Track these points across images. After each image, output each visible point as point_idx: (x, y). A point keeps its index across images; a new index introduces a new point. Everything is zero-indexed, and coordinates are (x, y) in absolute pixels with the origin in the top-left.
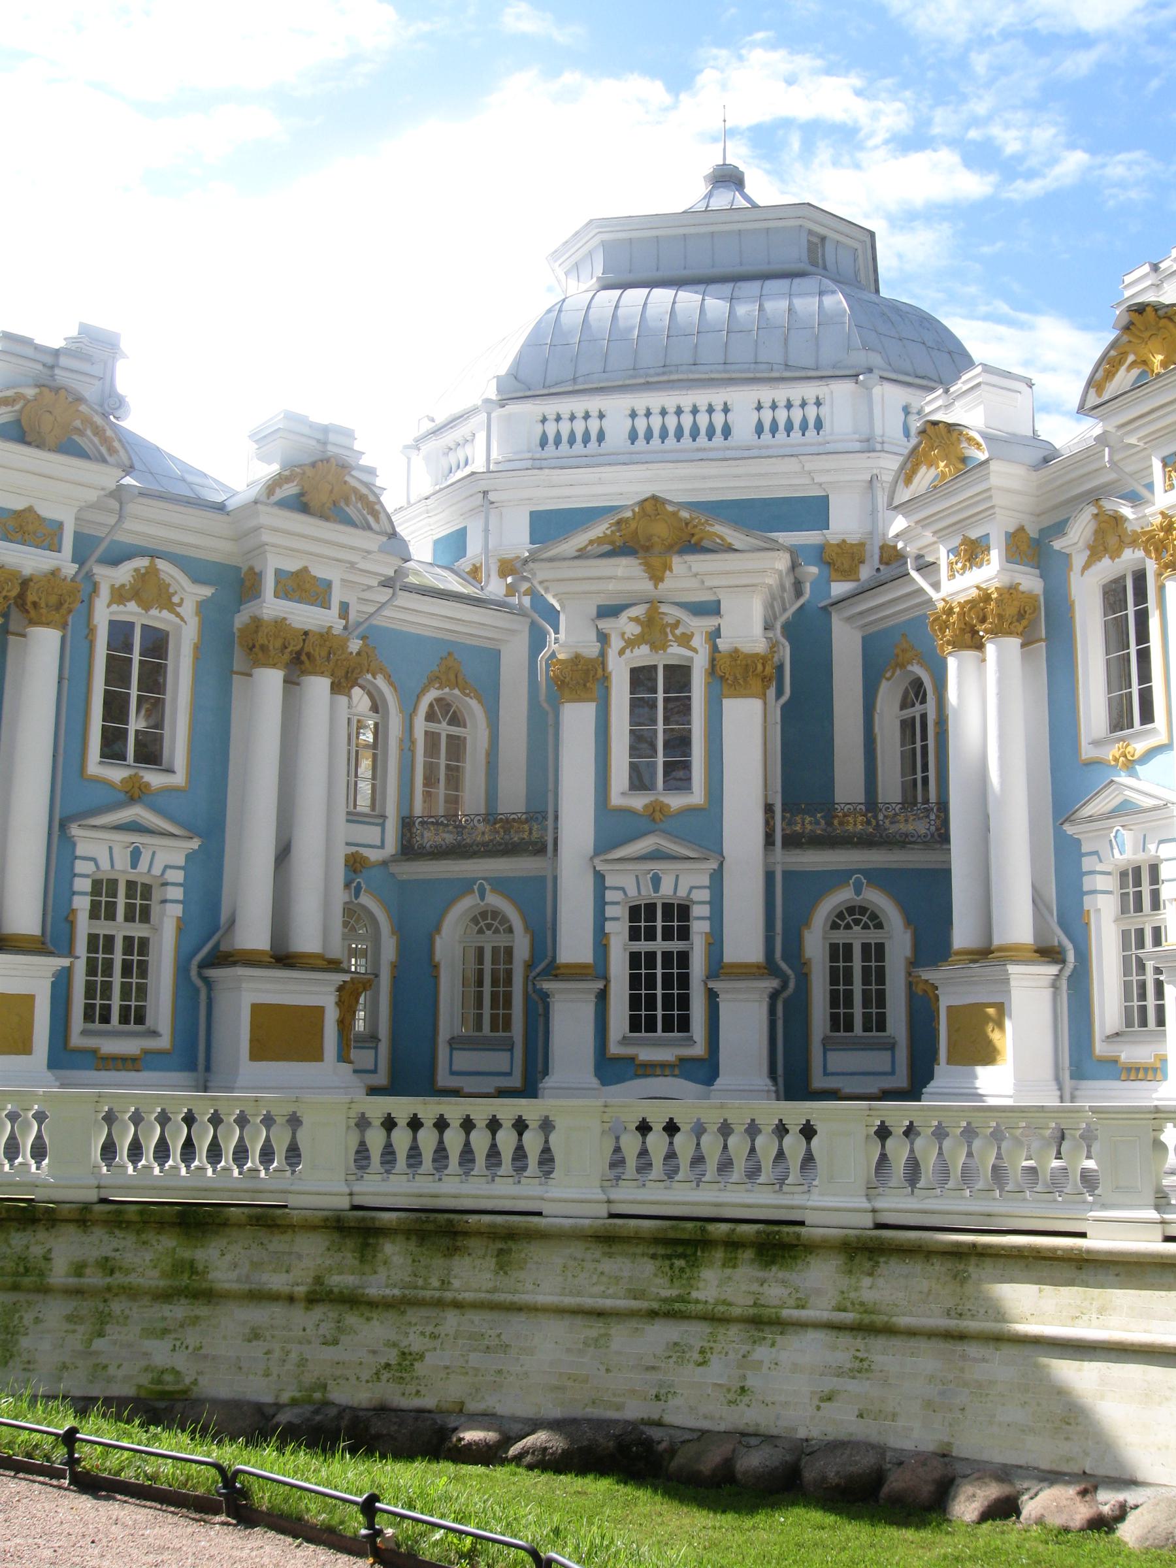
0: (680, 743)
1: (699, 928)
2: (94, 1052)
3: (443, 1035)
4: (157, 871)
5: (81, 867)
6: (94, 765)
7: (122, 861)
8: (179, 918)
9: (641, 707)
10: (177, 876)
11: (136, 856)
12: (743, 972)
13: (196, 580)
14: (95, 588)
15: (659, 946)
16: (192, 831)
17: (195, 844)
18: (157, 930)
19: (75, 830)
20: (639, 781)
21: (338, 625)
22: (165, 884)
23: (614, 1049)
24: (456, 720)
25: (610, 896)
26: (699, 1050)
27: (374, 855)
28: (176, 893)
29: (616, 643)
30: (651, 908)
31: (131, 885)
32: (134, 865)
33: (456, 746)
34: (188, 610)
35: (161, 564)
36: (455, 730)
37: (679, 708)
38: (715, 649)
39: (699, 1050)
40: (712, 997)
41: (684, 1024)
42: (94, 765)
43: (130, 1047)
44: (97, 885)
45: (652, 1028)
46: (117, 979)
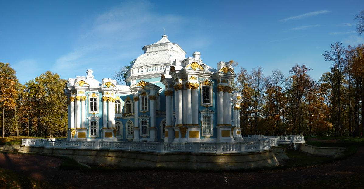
0: (146, 105)
1: (148, 123)
3: (127, 134)
9: (143, 101)
12: (152, 127)
15: (145, 125)
20: (143, 108)
22: (97, 122)
23: (141, 135)
24: (130, 102)
25: (140, 120)
26: (148, 136)
27: (120, 117)
29: (140, 95)
30: (144, 121)
33: (130, 105)
36: (129, 104)
37: (146, 101)
38: (149, 95)
39: (148, 136)
40: (149, 130)
41: (147, 134)
45: (144, 134)
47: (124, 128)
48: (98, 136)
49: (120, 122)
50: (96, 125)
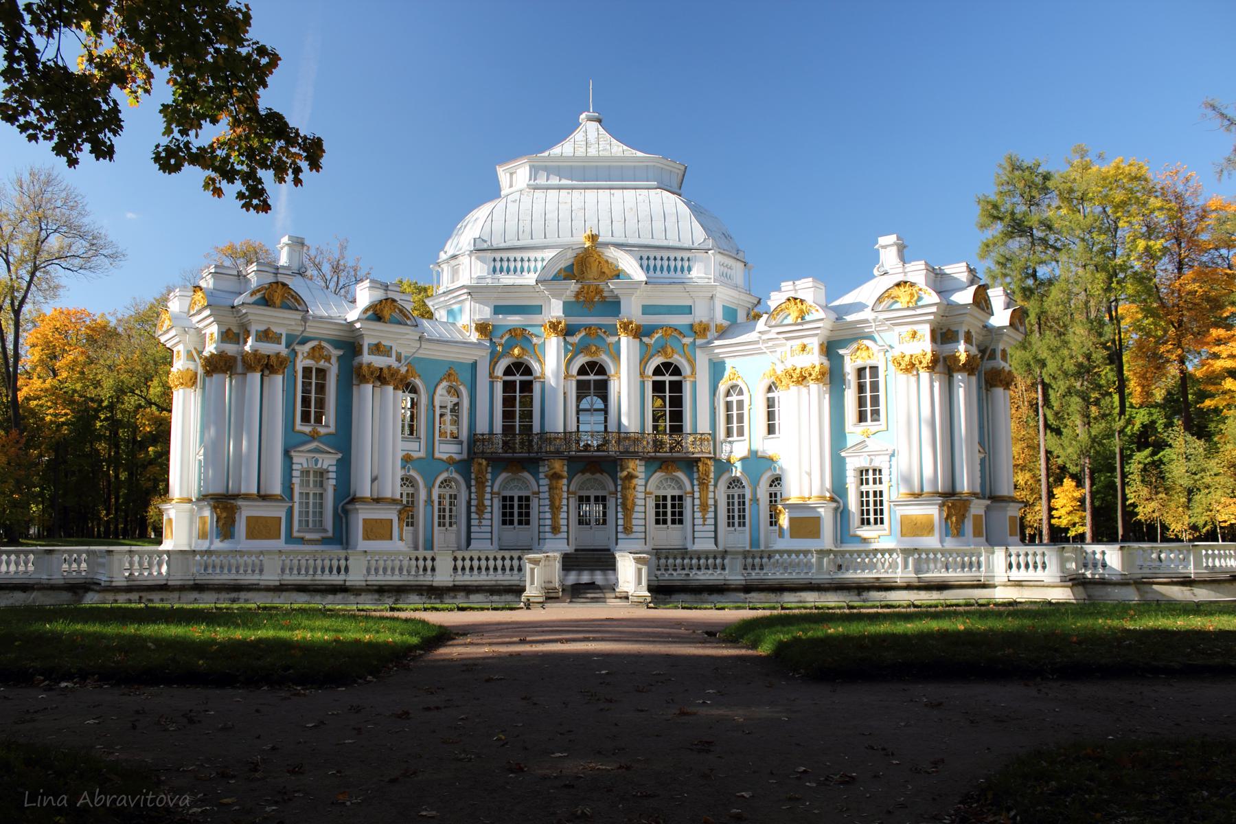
6: (299, 426)
8: (335, 486)
10: (334, 468)
11: (317, 461)
13: (336, 348)
14: (296, 354)
16: (338, 449)
17: (340, 456)
18: (325, 490)
19: (293, 454)
21: (395, 365)
22: (328, 472)
28: (333, 475)
31: (315, 472)
34: (334, 360)
35: (323, 344)
42: (299, 426)
44: (302, 472)
47: (429, 501)
48: (330, 534)
49: (412, 473)
50: (321, 486)
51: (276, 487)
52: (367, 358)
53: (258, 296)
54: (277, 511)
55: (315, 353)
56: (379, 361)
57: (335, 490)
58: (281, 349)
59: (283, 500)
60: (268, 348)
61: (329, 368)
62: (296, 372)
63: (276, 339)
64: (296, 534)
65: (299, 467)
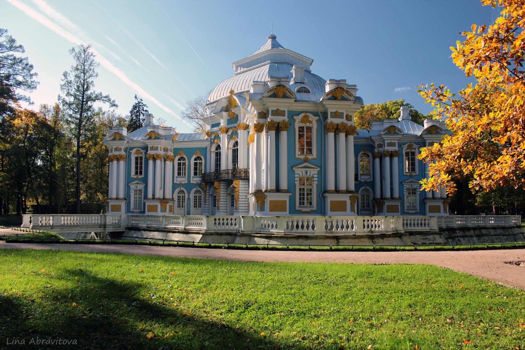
2: (301, 211)
4: (311, 175)
5: (296, 176)
7: (304, 174)
10: (316, 176)
11: (306, 172)
19: (294, 169)
28: (316, 179)
32: (306, 174)
34: (314, 122)
43: (308, 210)
44: (300, 180)
46: (305, 197)
51: (284, 185)
52: (330, 120)
53: (272, 93)
54: (285, 197)
55: (305, 119)
56: (337, 121)
57: (317, 186)
58: (286, 118)
59: (287, 191)
60: (278, 119)
61: (313, 127)
62: (295, 129)
63: (282, 113)
64: (297, 208)
65: (297, 176)
